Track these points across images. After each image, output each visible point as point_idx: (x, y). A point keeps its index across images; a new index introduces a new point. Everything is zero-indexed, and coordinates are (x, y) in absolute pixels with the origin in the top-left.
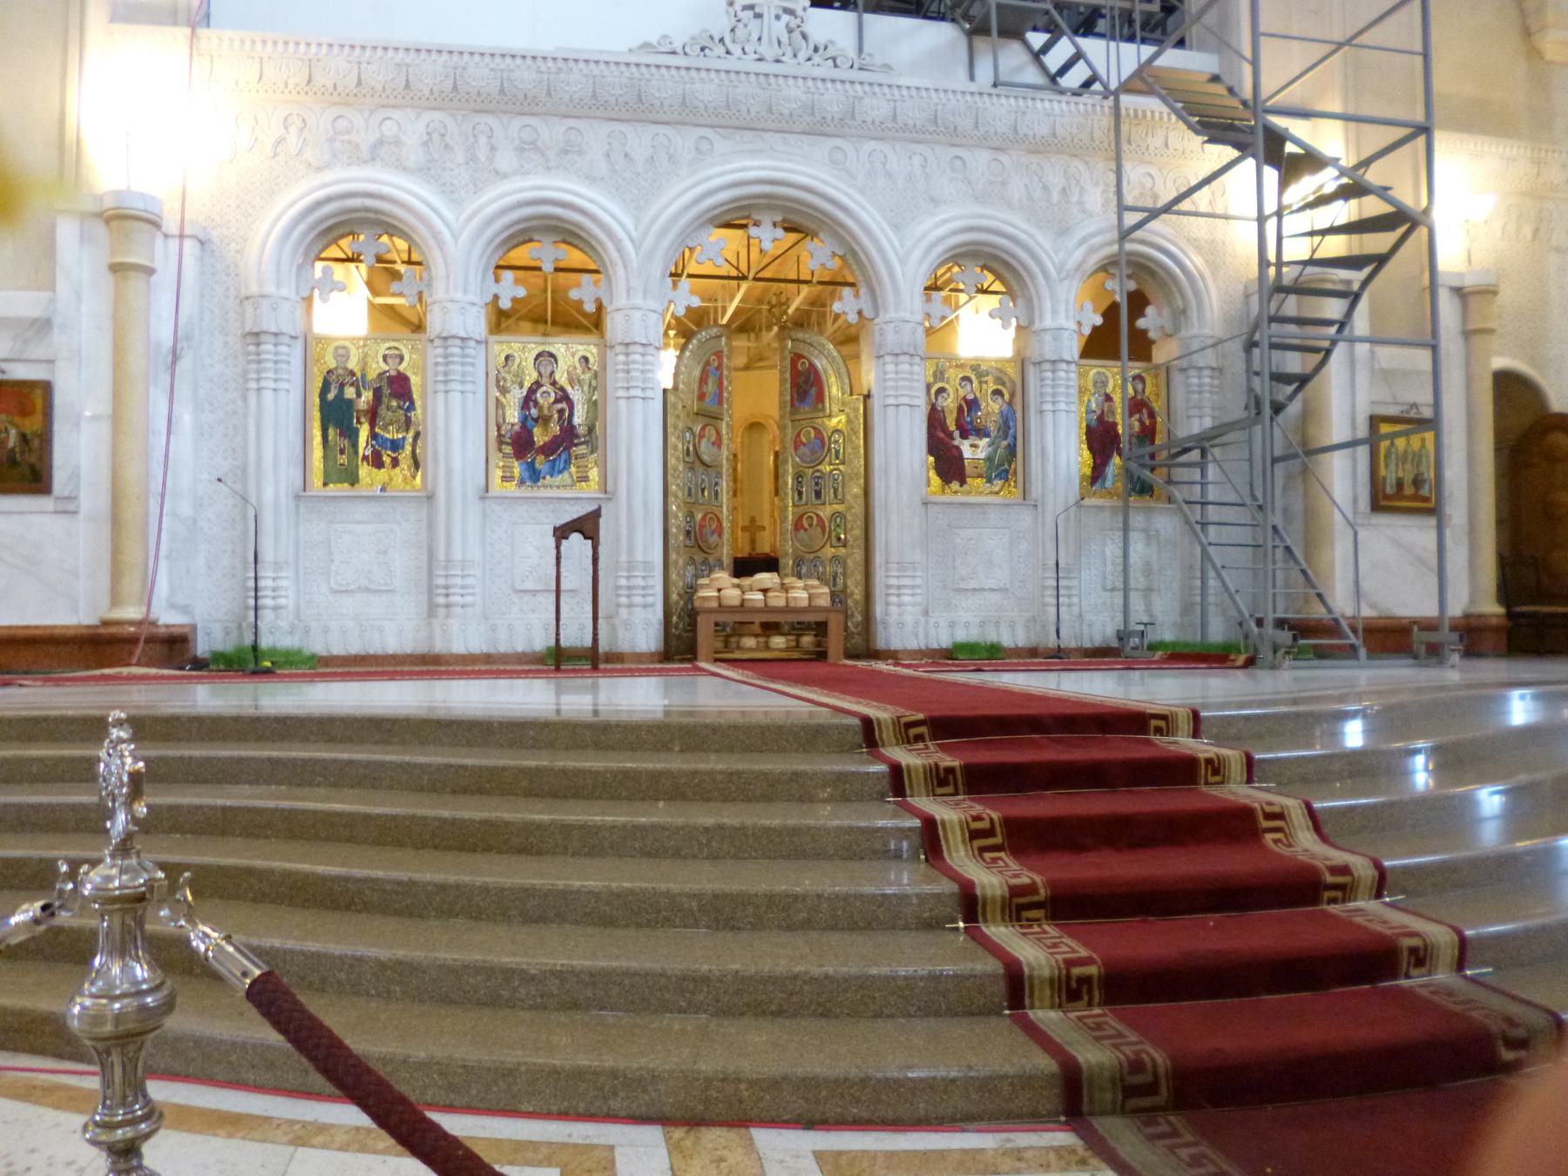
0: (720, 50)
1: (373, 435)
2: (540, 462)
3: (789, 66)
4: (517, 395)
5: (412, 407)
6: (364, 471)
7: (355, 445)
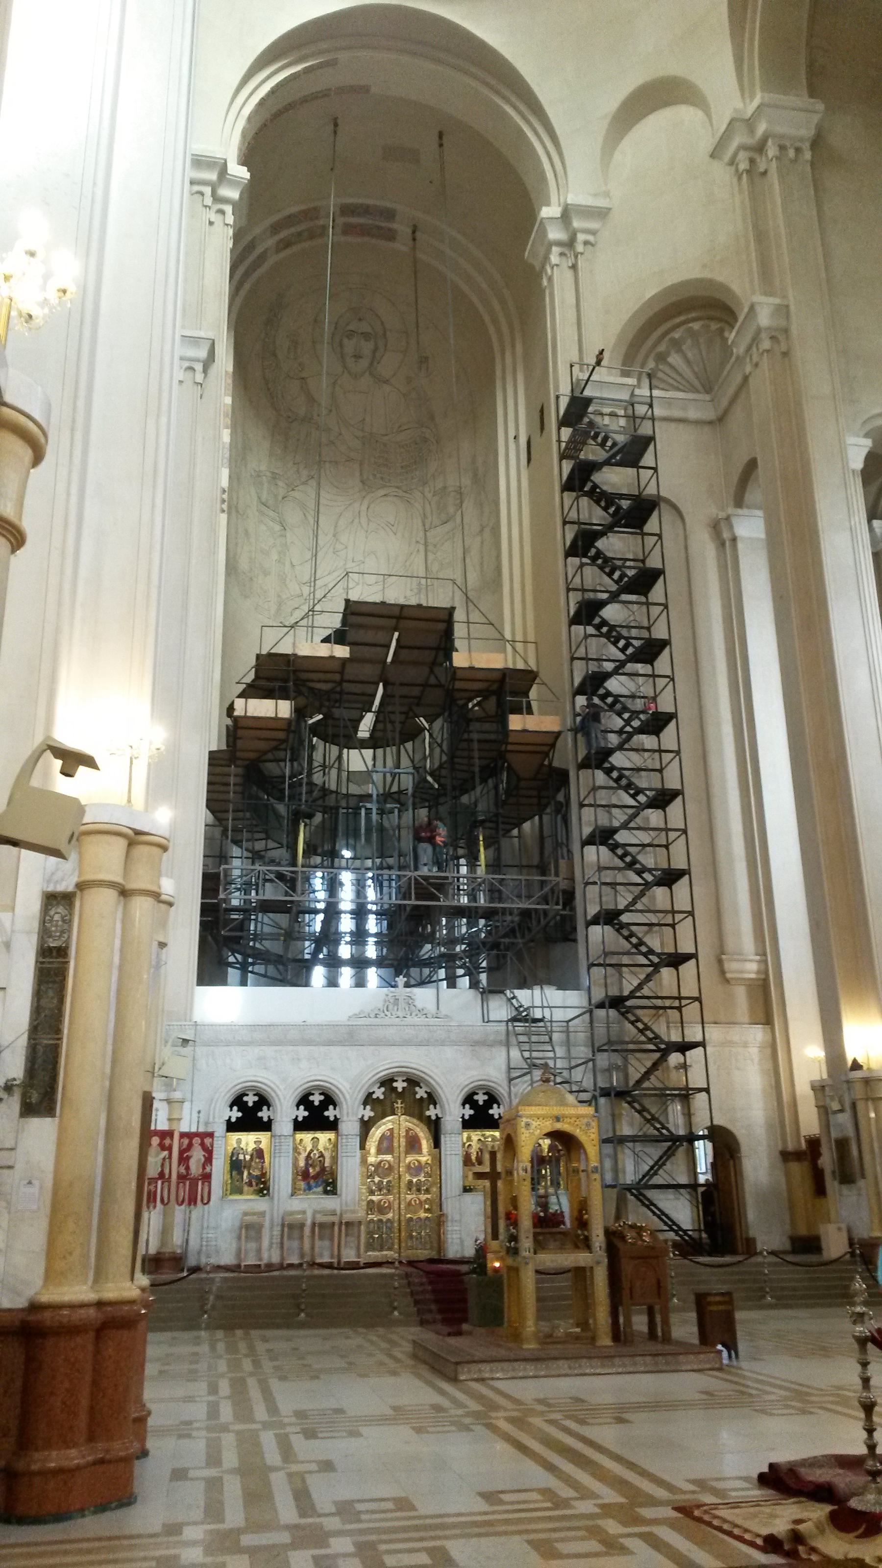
0: (382, 1015)
1: (249, 1174)
2: (312, 1182)
3: (409, 1020)
4: (304, 1155)
5: (264, 1162)
6: (246, 1188)
7: (242, 1178)
